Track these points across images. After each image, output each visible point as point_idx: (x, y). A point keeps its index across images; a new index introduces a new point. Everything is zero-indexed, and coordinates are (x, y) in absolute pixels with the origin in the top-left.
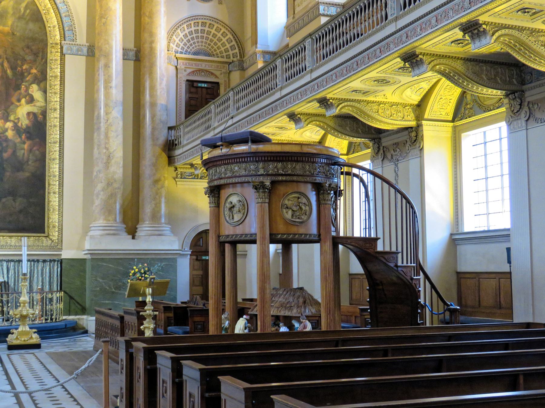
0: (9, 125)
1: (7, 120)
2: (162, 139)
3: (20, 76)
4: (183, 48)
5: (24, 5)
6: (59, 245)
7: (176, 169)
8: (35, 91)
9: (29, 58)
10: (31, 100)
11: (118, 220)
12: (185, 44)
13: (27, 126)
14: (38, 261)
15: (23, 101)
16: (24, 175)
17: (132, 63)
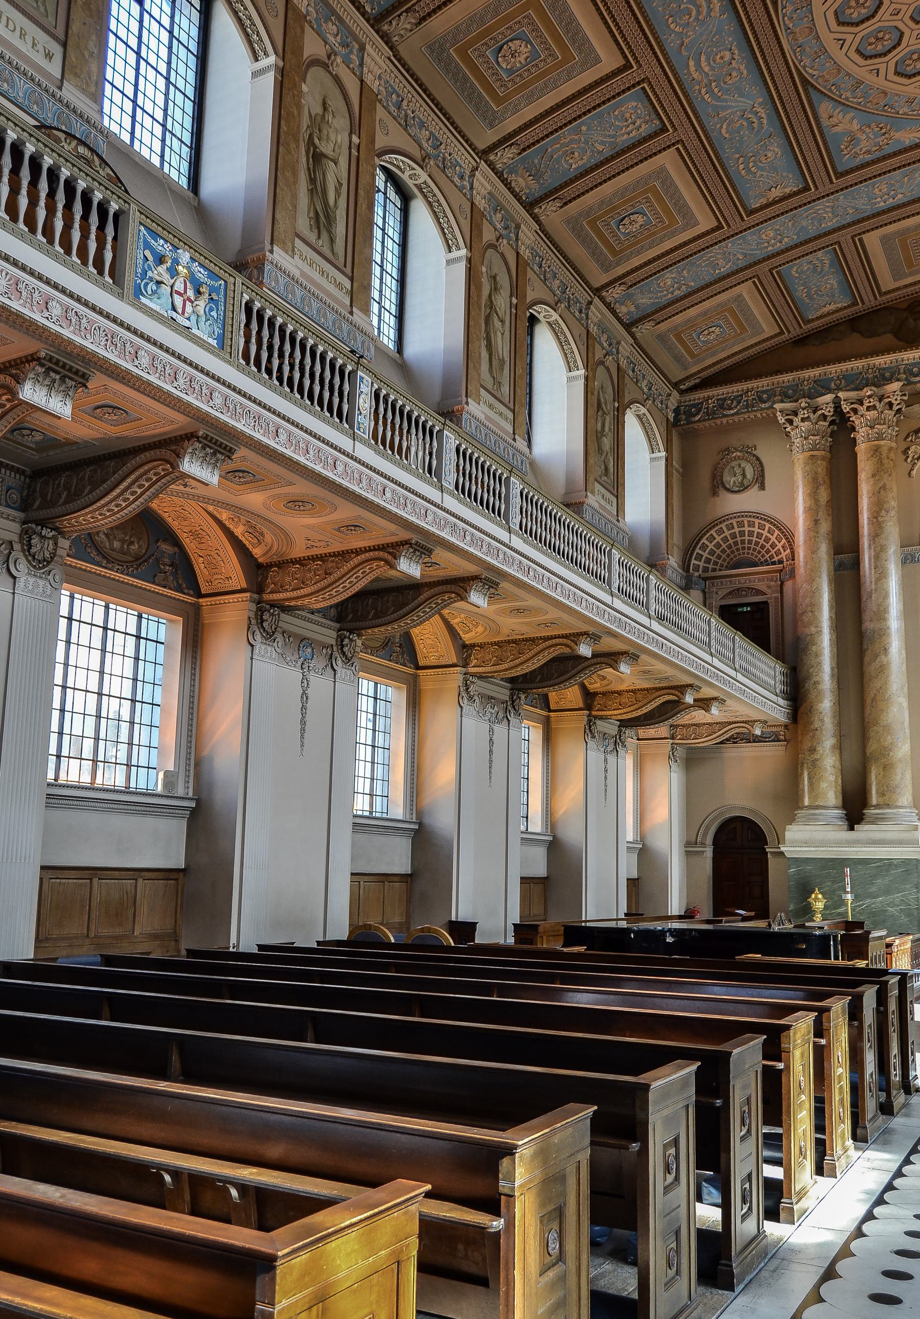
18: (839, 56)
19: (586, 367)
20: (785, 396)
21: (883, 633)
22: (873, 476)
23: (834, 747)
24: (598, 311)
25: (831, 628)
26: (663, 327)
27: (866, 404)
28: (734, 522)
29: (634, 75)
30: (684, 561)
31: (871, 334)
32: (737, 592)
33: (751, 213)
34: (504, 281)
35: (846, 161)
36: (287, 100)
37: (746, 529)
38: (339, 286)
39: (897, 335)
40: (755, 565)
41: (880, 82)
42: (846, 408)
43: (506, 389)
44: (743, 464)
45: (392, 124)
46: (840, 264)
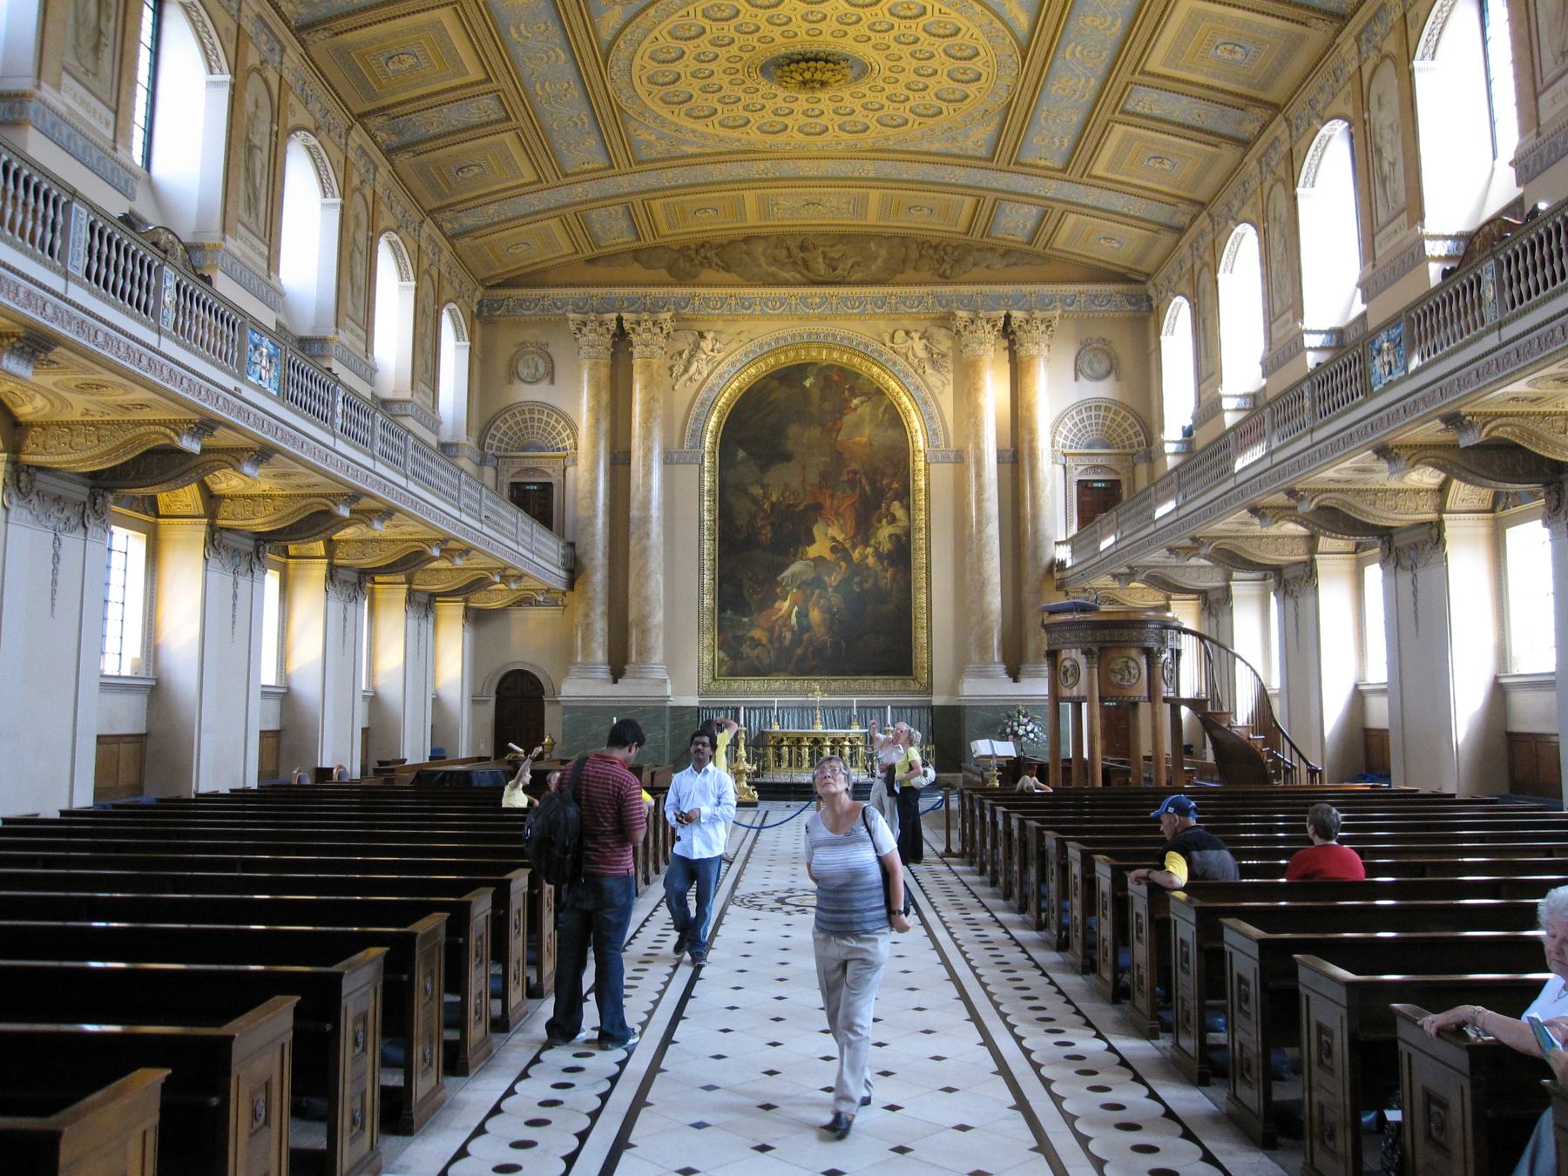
0: (870, 550)
1: (867, 545)
4: (1072, 441)
5: (882, 409)
6: (929, 689)
7: (1067, 594)
8: (897, 509)
10: (893, 520)
11: (996, 659)
12: (1075, 435)
13: (890, 552)
14: (906, 707)
15: (884, 521)
17: (1008, 467)
18: (647, 100)
19: (417, 279)
20: (577, 309)
21: (646, 520)
22: (646, 387)
23: (603, 613)
24: (428, 228)
25: (604, 512)
26: (479, 240)
27: (643, 325)
28: (526, 408)
29: (494, 85)
31: (650, 267)
32: (527, 471)
33: (567, 175)
34: (364, 219)
35: (645, 154)
36: (237, 109)
37: (536, 416)
38: (261, 254)
39: (670, 269)
40: (541, 449)
41: (674, 119)
42: (626, 326)
43: (361, 314)
44: (537, 358)
45: (299, 107)
46: (630, 214)
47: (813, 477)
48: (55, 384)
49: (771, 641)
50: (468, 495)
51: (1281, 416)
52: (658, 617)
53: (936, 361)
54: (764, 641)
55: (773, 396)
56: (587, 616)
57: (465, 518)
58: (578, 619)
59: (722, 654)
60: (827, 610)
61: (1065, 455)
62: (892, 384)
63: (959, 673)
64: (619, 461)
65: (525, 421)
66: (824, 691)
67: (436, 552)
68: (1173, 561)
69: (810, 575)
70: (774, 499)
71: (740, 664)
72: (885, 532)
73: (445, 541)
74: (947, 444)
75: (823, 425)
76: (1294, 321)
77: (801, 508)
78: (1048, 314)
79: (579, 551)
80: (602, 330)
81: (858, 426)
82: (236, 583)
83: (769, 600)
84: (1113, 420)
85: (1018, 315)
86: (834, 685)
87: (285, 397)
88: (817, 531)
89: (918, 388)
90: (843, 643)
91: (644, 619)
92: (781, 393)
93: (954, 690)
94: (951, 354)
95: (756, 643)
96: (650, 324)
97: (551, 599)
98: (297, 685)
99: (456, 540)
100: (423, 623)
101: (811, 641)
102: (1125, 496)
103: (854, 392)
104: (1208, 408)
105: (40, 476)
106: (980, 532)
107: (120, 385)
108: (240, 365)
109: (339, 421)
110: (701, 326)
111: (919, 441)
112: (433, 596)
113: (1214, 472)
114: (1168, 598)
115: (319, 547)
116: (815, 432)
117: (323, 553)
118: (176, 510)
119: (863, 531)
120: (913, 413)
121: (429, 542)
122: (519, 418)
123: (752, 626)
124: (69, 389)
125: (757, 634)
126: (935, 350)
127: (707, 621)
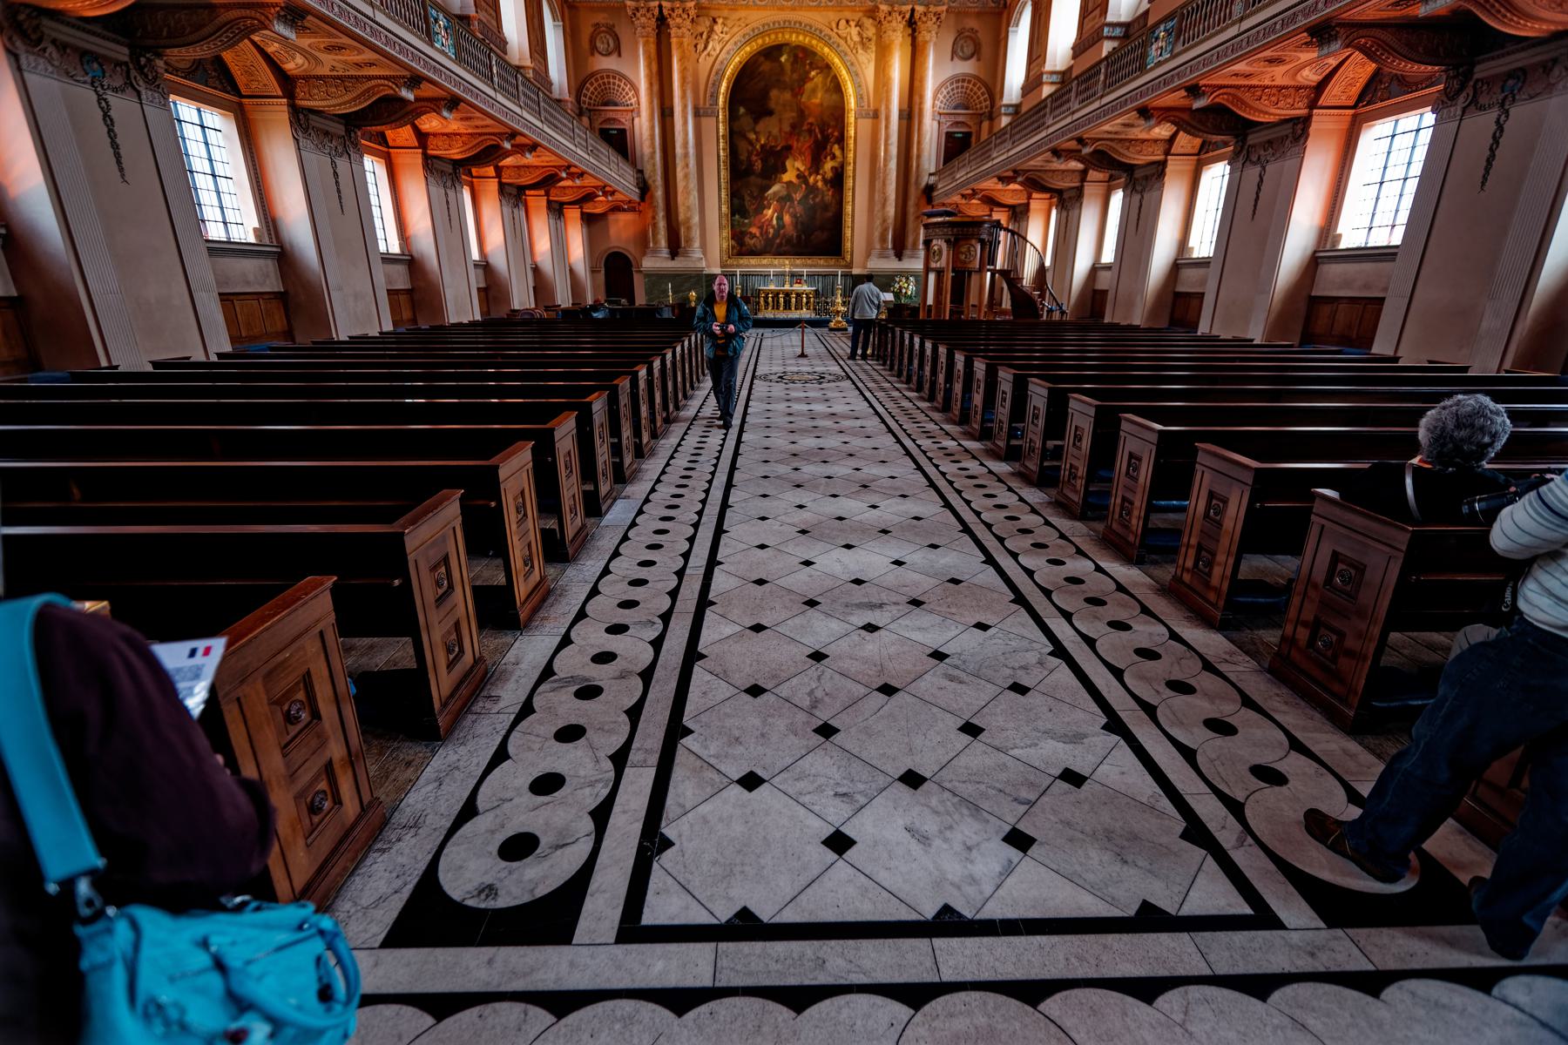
0: (819, 177)
1: (818, 174)
2: (923, 184)
3: (826, 139)
5: (829, 79)
6: (850, 265)
7: (933, 207)
8: (836, 150)
9: (832, 123)
10: (834, 157)
16: (830, 214)
17: (905, 122)
30: (577, 96)
40: (616, 105)
42: (666, 13)
47: (787, 128)
48: (309, 46)
49: (761, 234)
50: (579, 135)
51: (1083, 86)
52: (696, 219)
53: (864, 43)
54: (758, 234)
55: (761, 69)
56: (654, 218)
57: (579, 151)
58: (649, 220)
59: (734, 243)
60: (794, 216)
61: (940, 114)
62: (837, 61)
63: (868, 255)
64: (666, 113)
65: (604, 83)
66: (792, 265)
67: (564, 175)
68: (1000, 186)
69: (784, 193)
70: (762, 142)
71: (744, 249)
72: (828, 165)
73: (569, 167)
74: (869, 106)
75: (792, 90)
76: (1101, 16)
77: (779, 148)
78: (939, 9)
79: (646, 176)
80: (649, 15)
81: (814, 91)
82: (446, 194)
83: (760, 209)
84: (971, 90)
85: (920, 9)
86: (798, 262)
87: (459, 60)
88: (788, 163)
89: (852, 64)
90: (803, 237)
91: (688, 220)
92: (766, 66)
93: (865, 267)
94: (874, 38)
95: (753, 236)
96: (680, 11)
97: (632, 208)
98: (491, 261)
99: (576, 167)
100: (558, 222)
101: (784, 235)
102: (973, 145)
103: (813, 66)
104: (1032, 82)
105: (311, 116)
106: (885, 165)
107: (355, 48)
108: (428, 33)
109: (496, 79)
110: (714, 13)
111: (852, 103)
112: (562, 204)
113: (1036, 125)
114: (991, 210)
115: (491, 171)
116: (787, 95)
117: (494, 175)
118: (399, 143)
119: (816, 165)
120: (849, 82)
121: (558, 167)
122: (601, 82)
123: (750, 225)
124: (320, 50)
125: (754, 230)
126: (865, 36)
127: (724, 222)
